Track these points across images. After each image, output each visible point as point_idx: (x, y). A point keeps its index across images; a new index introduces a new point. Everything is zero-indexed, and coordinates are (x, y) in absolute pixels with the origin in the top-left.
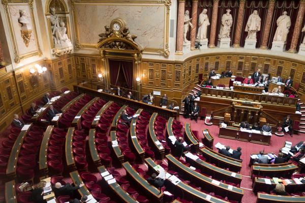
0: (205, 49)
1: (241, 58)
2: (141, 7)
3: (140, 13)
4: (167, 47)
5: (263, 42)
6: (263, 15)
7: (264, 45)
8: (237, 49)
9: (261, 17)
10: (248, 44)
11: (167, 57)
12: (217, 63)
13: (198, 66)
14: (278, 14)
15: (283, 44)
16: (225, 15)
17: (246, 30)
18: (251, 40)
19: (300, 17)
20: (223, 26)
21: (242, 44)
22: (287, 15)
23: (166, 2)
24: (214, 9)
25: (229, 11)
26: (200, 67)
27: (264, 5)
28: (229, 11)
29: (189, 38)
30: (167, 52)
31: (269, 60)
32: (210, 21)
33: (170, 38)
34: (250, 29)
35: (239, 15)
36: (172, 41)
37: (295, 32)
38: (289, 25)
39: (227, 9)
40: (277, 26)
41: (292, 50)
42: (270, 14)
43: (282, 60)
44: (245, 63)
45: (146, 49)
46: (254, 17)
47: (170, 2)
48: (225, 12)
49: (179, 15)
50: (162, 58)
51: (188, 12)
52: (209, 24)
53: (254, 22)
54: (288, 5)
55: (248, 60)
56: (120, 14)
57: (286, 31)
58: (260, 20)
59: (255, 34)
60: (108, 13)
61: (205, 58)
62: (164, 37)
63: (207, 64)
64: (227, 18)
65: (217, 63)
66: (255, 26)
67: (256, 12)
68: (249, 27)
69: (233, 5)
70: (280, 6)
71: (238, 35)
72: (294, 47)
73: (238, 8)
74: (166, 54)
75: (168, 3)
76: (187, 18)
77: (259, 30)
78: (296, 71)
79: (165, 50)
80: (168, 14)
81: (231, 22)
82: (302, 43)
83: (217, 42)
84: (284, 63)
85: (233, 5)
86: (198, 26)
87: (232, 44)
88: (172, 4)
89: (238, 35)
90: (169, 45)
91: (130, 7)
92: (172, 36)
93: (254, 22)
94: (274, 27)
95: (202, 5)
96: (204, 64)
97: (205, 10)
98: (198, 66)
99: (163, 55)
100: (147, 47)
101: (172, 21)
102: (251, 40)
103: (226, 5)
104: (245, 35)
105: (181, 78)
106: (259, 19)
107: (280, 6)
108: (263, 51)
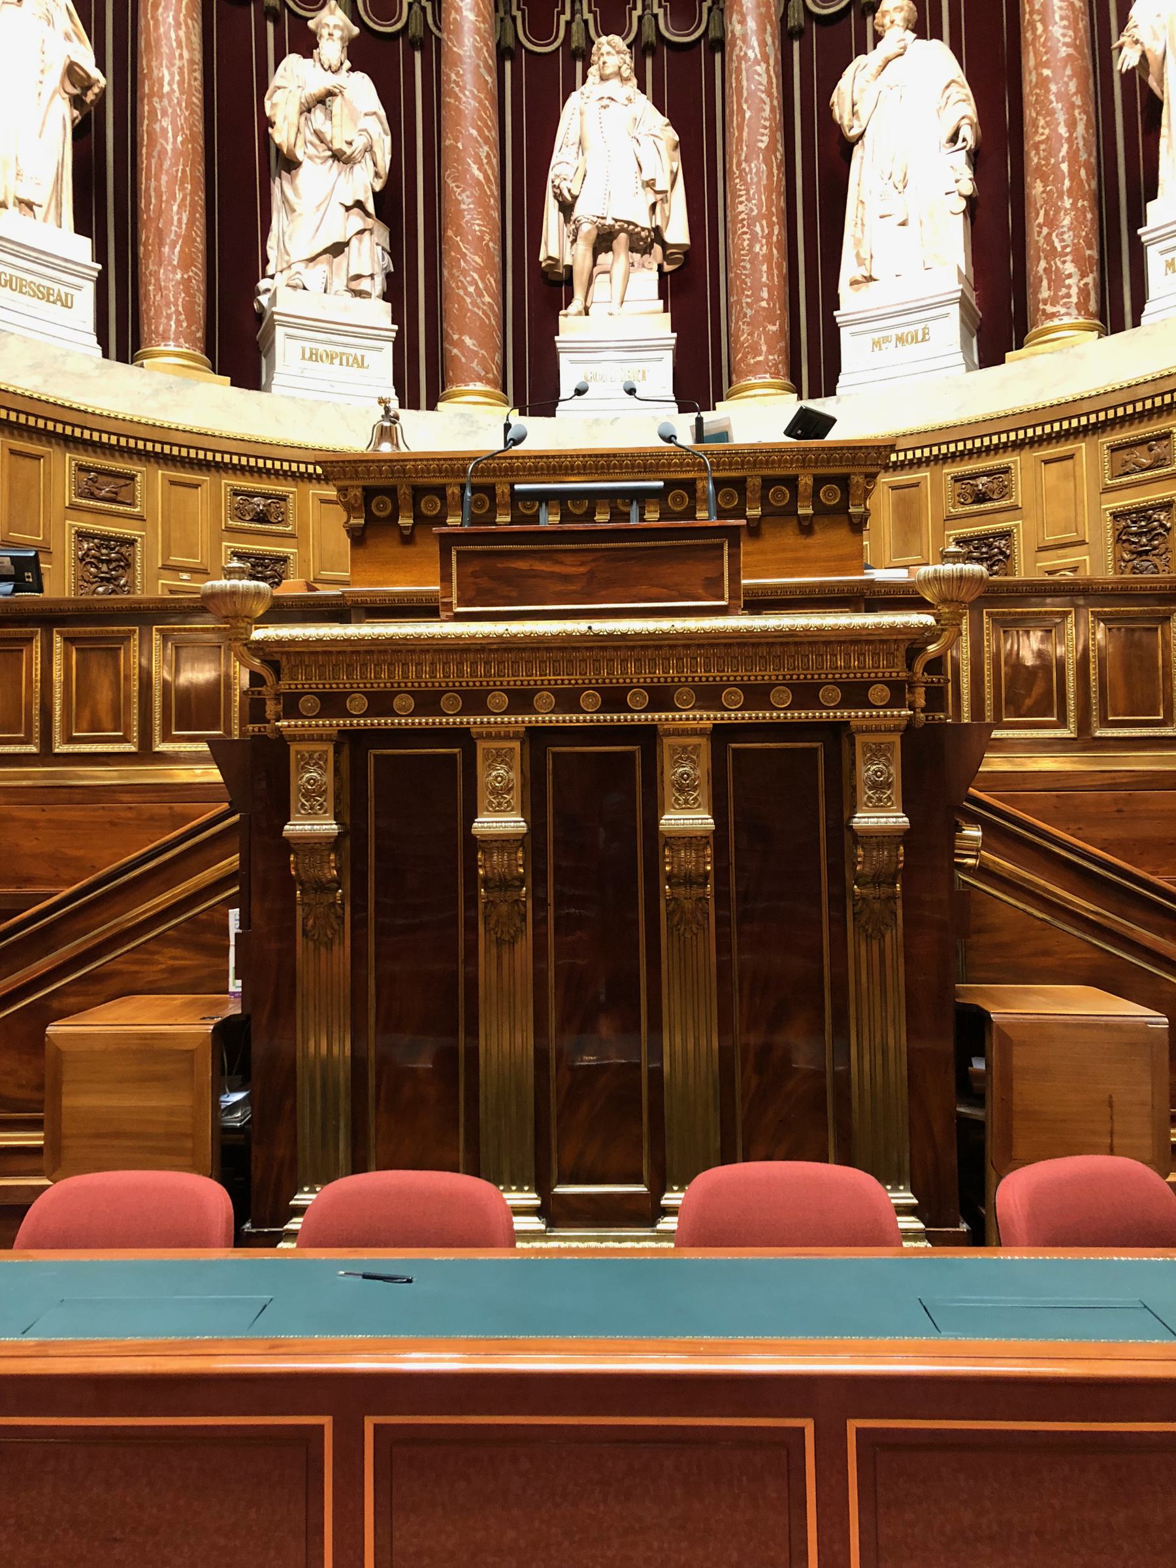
9: (675, 123)
16: (293, 61)
18: (617, 333)
20: (290, 164)
25: (333, 25)
38: (962, 108)
48: (306, 43)
53: (614, 145)
58: (672, 135)
61: (63, 466)
68: (566, 208)
71: (474, 284)
77: (678, 233)
83: (237, 345)
84: (1020, 483)
87: (421, 375)
94: (822, 162)
102: (617, 333)
104: (540, 295)
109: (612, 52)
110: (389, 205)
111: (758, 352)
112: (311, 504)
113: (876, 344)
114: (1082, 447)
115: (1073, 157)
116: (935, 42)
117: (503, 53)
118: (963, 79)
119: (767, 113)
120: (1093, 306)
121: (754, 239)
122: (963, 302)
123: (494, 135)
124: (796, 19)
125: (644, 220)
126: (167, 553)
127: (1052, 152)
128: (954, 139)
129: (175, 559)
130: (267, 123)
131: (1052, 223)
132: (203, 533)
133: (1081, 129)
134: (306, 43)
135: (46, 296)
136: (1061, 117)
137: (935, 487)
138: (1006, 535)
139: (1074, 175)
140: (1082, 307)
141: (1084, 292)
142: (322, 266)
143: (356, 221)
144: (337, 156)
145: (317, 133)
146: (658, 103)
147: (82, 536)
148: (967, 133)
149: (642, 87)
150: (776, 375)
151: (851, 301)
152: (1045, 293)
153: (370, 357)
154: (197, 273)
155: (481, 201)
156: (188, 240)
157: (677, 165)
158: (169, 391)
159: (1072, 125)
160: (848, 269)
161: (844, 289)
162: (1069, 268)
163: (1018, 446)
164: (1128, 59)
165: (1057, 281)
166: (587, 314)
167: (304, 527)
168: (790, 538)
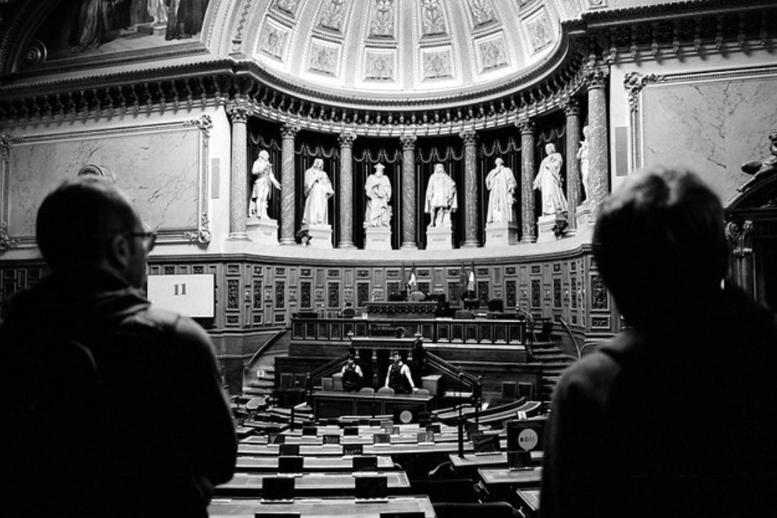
0: (320, 247)
1: (424, 274)
2: (148, 138)
3: (147, 151)
4: (205, 223)
5: (467, 232)
6: (457, 174)
7: (470, 239)
8: (409, 253)
10: (435, 240)
11: (205, 245)
12: (363, 289)
13: (306, 287)
14: (485, 166)
15: (507, 226)
16: (371, 176)
17: (426, 210)
19: (526, 163)
20: (370, 199)
21: (421, 242)
22: (506, 164)
23: (201, 122)
24: (342, 161)
25: (380, 167)
26: (314, 293)
27: (458, 154)
28: (380, 167)
29: (274, 210)
30: (204, 234)
31: (485, 272)
32: (336, 184)
33: (211, 202)
34: (434, 204)
35: (405, 175)
36: (218, 211)
37: (523, 197)
38: (512, 185)
39: (376, 164)
40: (489, 192)
41: (527, 237)
42: (470, 168)
43: (510, 264)
44: (435, 287)
45: (164, 232)
46: (438, 179)
47: (210, 122)
48: (373, 171)
49: (233, 149)
50: (193, 250)
51: (264, 154)
52: (332, 192)
53: (440, 188)
54: (504, 148)
55: (439, 277)
56: (104, 157)
57: (510, 200)
58: (454, 184)
59: (448, 216)
60: (78, 158)
61: (326, 270)
62: (197, 199)
63: (334, 287)
64: (378, 184)
65: (363, 289)
66: (441, 198)
67: (439, 168)
69: (391, 157)
70: (489, 151)
71: (409, 221)
72: (529, 230)
73: (400, 163)
74: (203, 238)
75: (205, 123)
76: (263, 163)
77: (455, 205)
78: (541, 284)
79: (201, 228)
80: (206, 146)
81: (389, 191)
82: (541, 215)
83: (359, 239)
84: (517, 270)
85: (391, 157)
86: (301, 196)
87: (396, 244)
88: (214, 123)
89: (409, 221)
90: (210, 217)
91: (126, 140)
92: (216, 196)
93: (440, 188)
94: (483, 196)
95: (313, 151)
96: (327, 286)
97: (319, 162)
98: (306, 287)
99: (196, 243)
100: (160, 227)
101: (216, 161)
102: (441, 228)
103: (374, 157)
104: (424, 220)
105: (241, 301)
106: (450, 183)
107: (489, 150)
108: (470, 252)
109: (439, 168)
110: (392, 202)
111: (469, 235)
112: (374, 273)
113: (493, 236)
114: (527, 265)
115: (529, 202)
116: (508, 169)
117: (416, 164)
118: (513, 177)
119: (472, 181)
120: (533, 233)
121: (469, 210)
122: (510, 230)
123: (413, 186)
124: (482, 156)
125: (446, 205)
126: (345, 284)
127: (525, 201)
128: (510, 191)
129: (347, 285)
130: (365, 191)
131: (525, 216)
132: (352, 280)
133: (531, 196)
134: (373, 171)
135: (323, 238)
136: (526, 193)
137: (503, 269)
138: (514, 282)
139: (529, 206)
140: (531, 234)
141: (531, 231)
142: (376, 221)
143: (384, 210)
144: (379, 197)
145: (376, 193)
146: (452, 178)
147: (330, 283)
148: (513, 191)
149: (448, 174)
150: (473, 239)
151: (488, 227)
152: (523, 230)
153: (386, 239)
154: (351, 227)
155: (411, 202)
156: (349, 220)
157: (454, 190)
158: (348, 253)
159: (529, 195)
160: (489, 219)
161: (487, 224)
162: (528, 226)
163: (517, 263)
164: (535, 188)
165: (526, 228)
166: (434, 225)
167: (372, 276)
168: (425, 314)
